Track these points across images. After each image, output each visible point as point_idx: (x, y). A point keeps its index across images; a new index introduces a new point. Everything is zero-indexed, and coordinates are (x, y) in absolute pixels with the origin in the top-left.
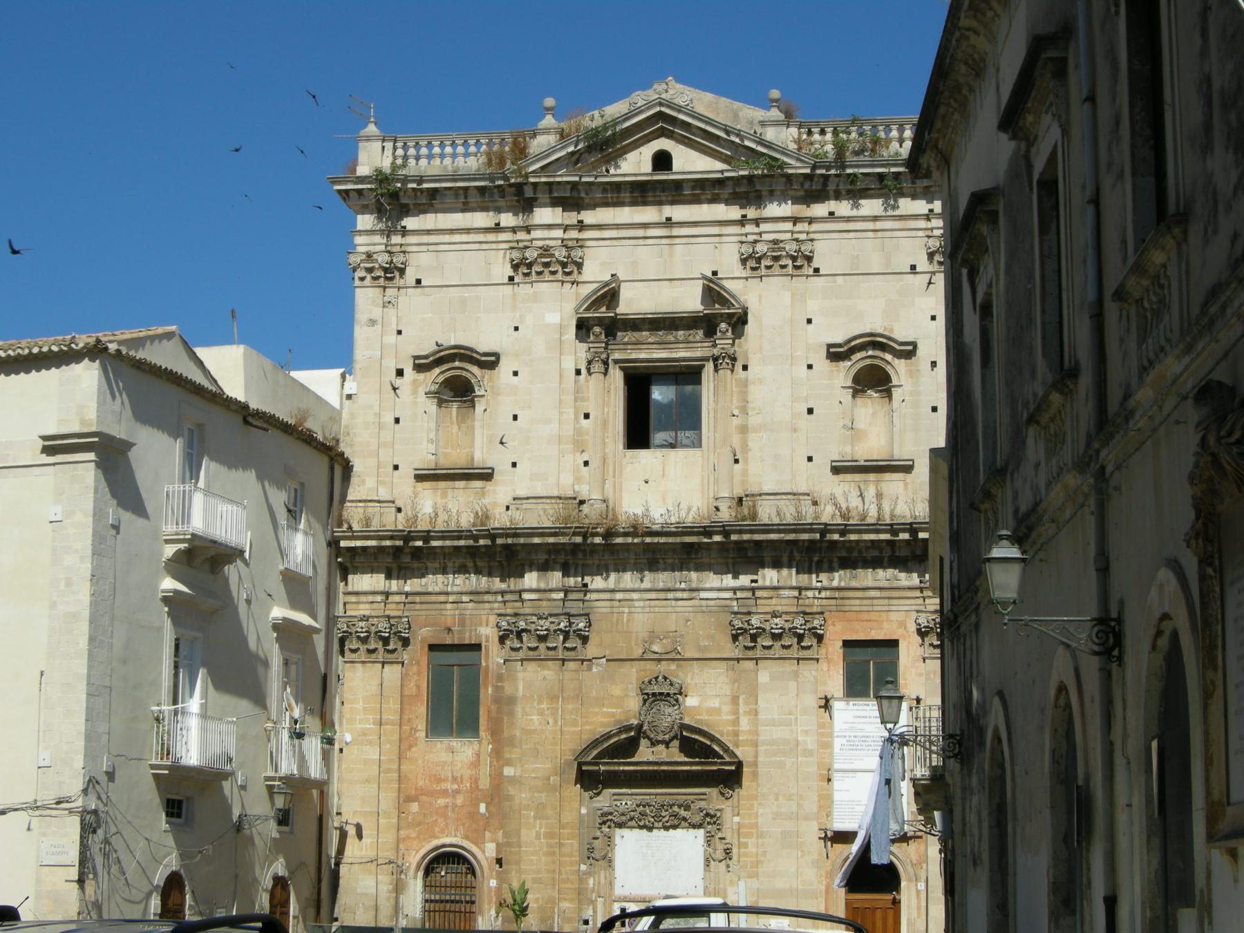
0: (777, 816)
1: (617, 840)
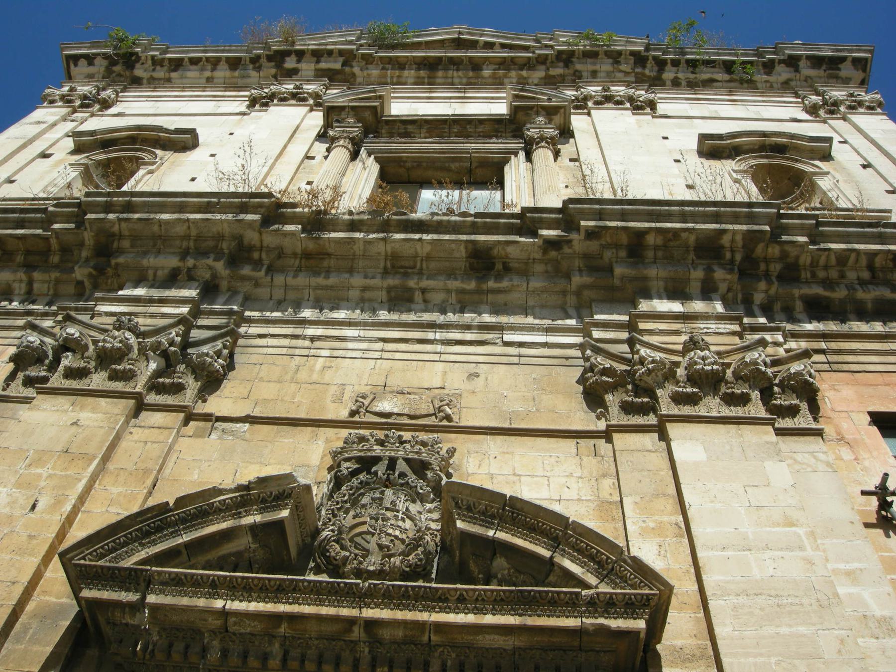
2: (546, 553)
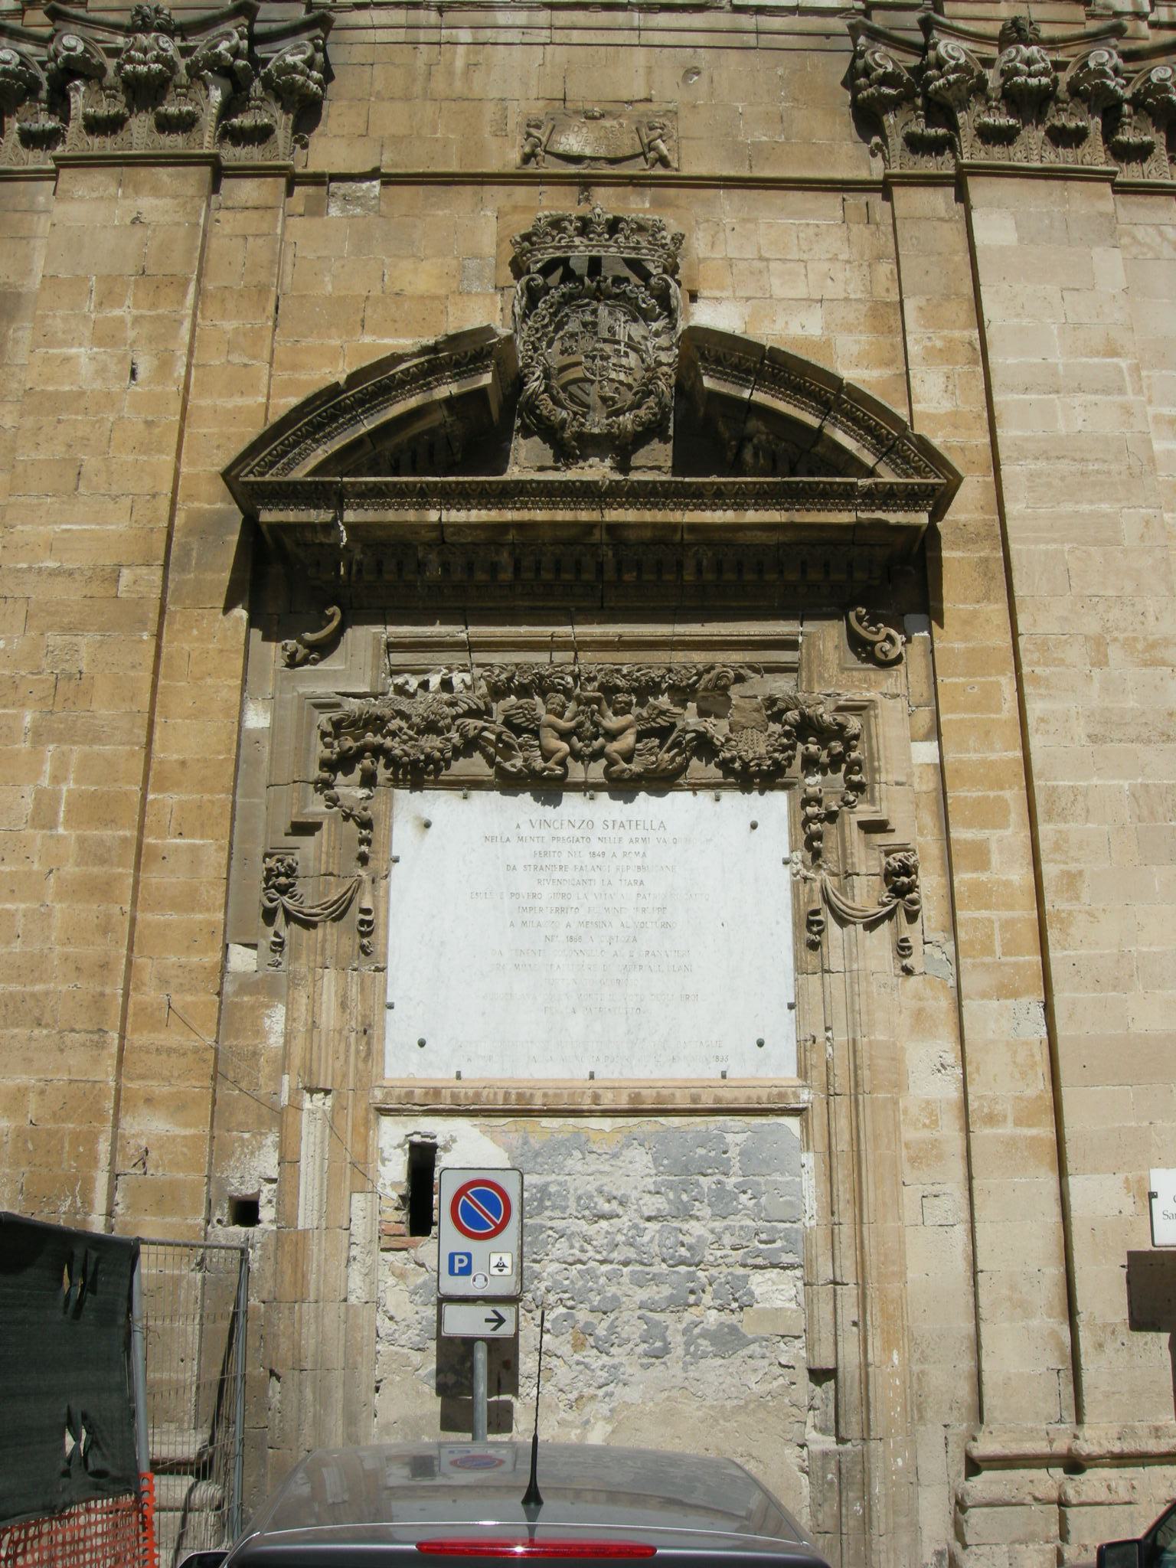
0: (1104, 731)
1: (402, 836)
2: (813, 421)
